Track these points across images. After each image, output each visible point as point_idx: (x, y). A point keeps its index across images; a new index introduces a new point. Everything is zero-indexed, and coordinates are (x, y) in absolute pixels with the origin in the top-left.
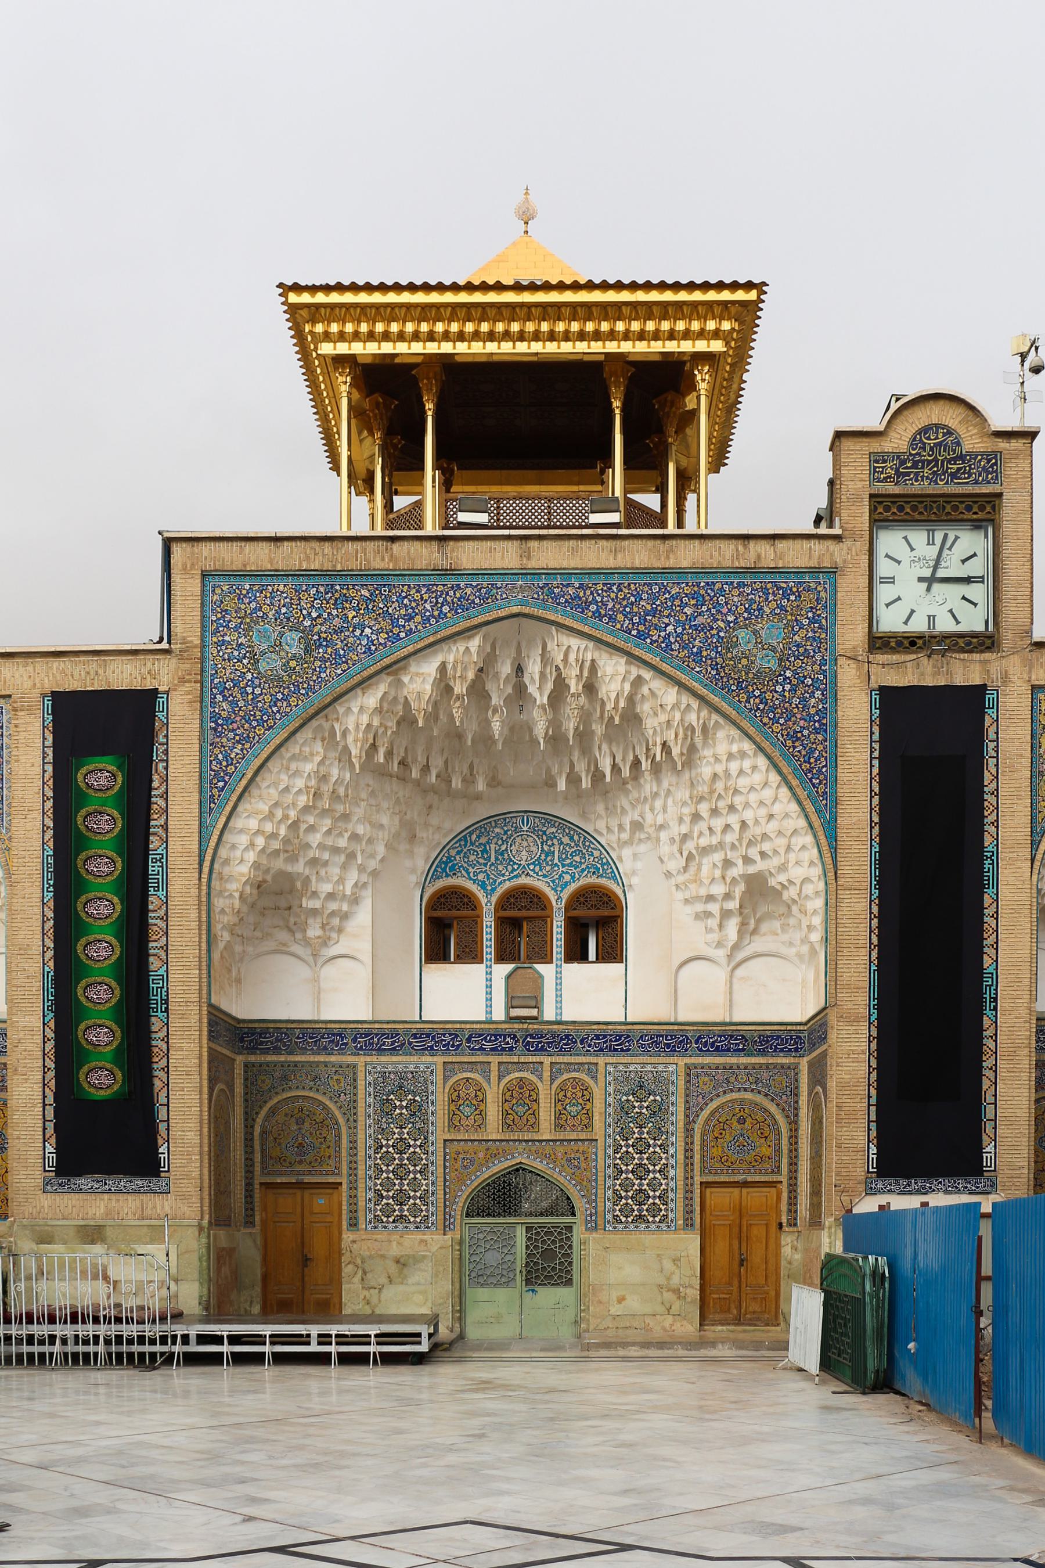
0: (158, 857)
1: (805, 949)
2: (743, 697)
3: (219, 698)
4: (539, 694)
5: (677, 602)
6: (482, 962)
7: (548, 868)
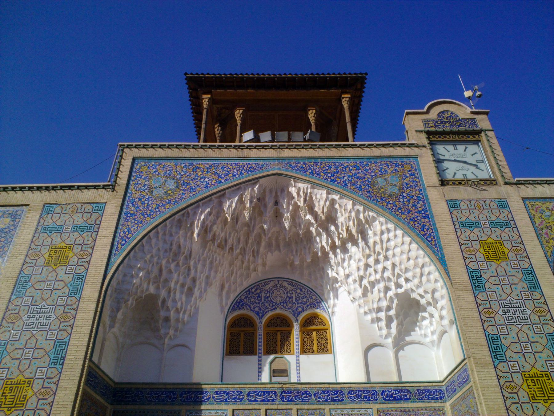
0: (81, 277)
2: (385, 204)
3: (131, 205)
6: (256, 355)
7: (290, 305)
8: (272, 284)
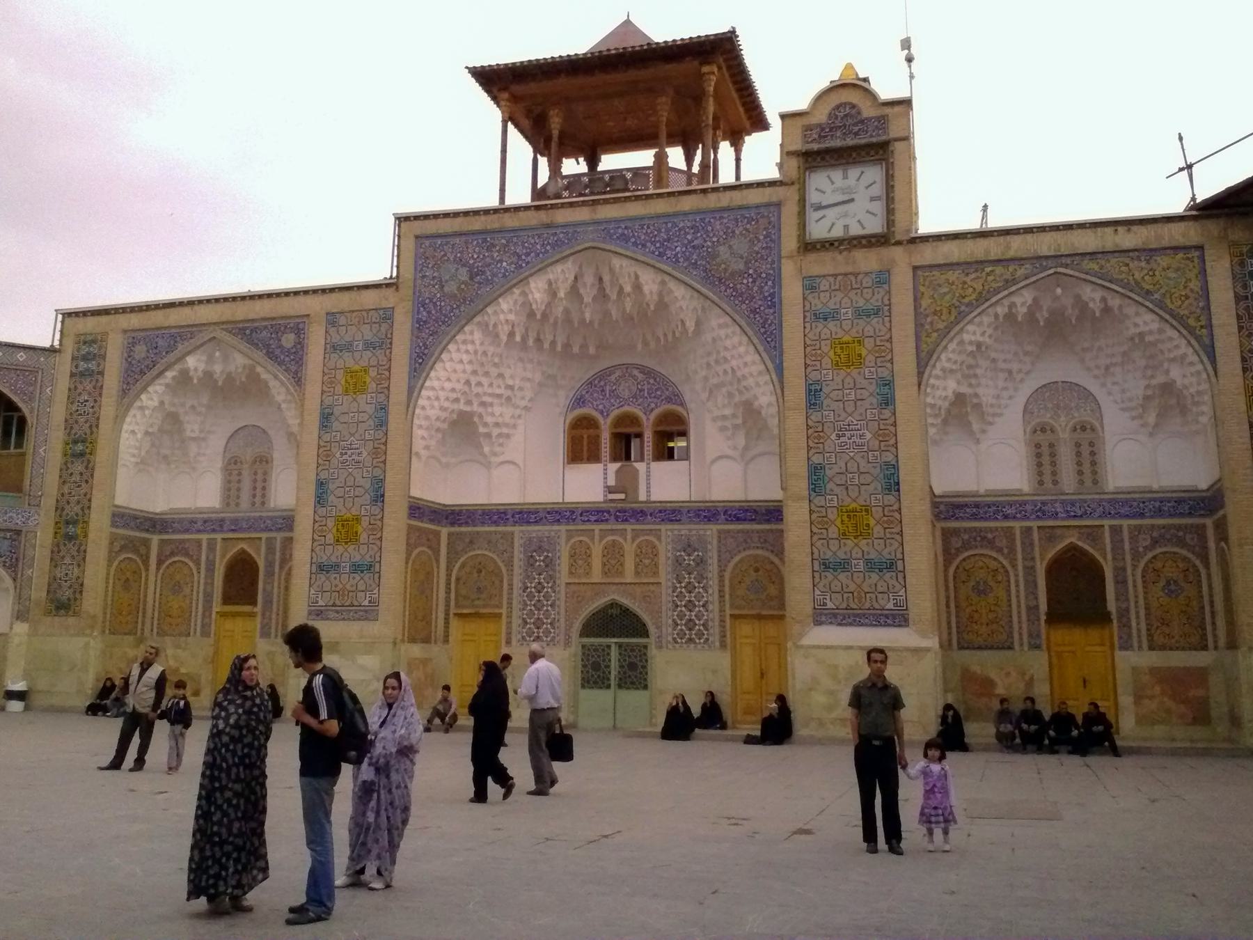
2: (723, 288)
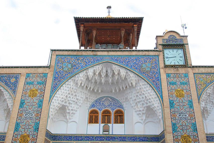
1: (158, 120)
2: (145, 75)
3: (56, 74)
4: (110, 75)
5: (133, 60)
8: (105, 99)
